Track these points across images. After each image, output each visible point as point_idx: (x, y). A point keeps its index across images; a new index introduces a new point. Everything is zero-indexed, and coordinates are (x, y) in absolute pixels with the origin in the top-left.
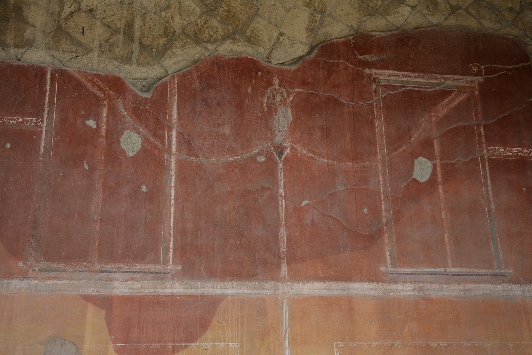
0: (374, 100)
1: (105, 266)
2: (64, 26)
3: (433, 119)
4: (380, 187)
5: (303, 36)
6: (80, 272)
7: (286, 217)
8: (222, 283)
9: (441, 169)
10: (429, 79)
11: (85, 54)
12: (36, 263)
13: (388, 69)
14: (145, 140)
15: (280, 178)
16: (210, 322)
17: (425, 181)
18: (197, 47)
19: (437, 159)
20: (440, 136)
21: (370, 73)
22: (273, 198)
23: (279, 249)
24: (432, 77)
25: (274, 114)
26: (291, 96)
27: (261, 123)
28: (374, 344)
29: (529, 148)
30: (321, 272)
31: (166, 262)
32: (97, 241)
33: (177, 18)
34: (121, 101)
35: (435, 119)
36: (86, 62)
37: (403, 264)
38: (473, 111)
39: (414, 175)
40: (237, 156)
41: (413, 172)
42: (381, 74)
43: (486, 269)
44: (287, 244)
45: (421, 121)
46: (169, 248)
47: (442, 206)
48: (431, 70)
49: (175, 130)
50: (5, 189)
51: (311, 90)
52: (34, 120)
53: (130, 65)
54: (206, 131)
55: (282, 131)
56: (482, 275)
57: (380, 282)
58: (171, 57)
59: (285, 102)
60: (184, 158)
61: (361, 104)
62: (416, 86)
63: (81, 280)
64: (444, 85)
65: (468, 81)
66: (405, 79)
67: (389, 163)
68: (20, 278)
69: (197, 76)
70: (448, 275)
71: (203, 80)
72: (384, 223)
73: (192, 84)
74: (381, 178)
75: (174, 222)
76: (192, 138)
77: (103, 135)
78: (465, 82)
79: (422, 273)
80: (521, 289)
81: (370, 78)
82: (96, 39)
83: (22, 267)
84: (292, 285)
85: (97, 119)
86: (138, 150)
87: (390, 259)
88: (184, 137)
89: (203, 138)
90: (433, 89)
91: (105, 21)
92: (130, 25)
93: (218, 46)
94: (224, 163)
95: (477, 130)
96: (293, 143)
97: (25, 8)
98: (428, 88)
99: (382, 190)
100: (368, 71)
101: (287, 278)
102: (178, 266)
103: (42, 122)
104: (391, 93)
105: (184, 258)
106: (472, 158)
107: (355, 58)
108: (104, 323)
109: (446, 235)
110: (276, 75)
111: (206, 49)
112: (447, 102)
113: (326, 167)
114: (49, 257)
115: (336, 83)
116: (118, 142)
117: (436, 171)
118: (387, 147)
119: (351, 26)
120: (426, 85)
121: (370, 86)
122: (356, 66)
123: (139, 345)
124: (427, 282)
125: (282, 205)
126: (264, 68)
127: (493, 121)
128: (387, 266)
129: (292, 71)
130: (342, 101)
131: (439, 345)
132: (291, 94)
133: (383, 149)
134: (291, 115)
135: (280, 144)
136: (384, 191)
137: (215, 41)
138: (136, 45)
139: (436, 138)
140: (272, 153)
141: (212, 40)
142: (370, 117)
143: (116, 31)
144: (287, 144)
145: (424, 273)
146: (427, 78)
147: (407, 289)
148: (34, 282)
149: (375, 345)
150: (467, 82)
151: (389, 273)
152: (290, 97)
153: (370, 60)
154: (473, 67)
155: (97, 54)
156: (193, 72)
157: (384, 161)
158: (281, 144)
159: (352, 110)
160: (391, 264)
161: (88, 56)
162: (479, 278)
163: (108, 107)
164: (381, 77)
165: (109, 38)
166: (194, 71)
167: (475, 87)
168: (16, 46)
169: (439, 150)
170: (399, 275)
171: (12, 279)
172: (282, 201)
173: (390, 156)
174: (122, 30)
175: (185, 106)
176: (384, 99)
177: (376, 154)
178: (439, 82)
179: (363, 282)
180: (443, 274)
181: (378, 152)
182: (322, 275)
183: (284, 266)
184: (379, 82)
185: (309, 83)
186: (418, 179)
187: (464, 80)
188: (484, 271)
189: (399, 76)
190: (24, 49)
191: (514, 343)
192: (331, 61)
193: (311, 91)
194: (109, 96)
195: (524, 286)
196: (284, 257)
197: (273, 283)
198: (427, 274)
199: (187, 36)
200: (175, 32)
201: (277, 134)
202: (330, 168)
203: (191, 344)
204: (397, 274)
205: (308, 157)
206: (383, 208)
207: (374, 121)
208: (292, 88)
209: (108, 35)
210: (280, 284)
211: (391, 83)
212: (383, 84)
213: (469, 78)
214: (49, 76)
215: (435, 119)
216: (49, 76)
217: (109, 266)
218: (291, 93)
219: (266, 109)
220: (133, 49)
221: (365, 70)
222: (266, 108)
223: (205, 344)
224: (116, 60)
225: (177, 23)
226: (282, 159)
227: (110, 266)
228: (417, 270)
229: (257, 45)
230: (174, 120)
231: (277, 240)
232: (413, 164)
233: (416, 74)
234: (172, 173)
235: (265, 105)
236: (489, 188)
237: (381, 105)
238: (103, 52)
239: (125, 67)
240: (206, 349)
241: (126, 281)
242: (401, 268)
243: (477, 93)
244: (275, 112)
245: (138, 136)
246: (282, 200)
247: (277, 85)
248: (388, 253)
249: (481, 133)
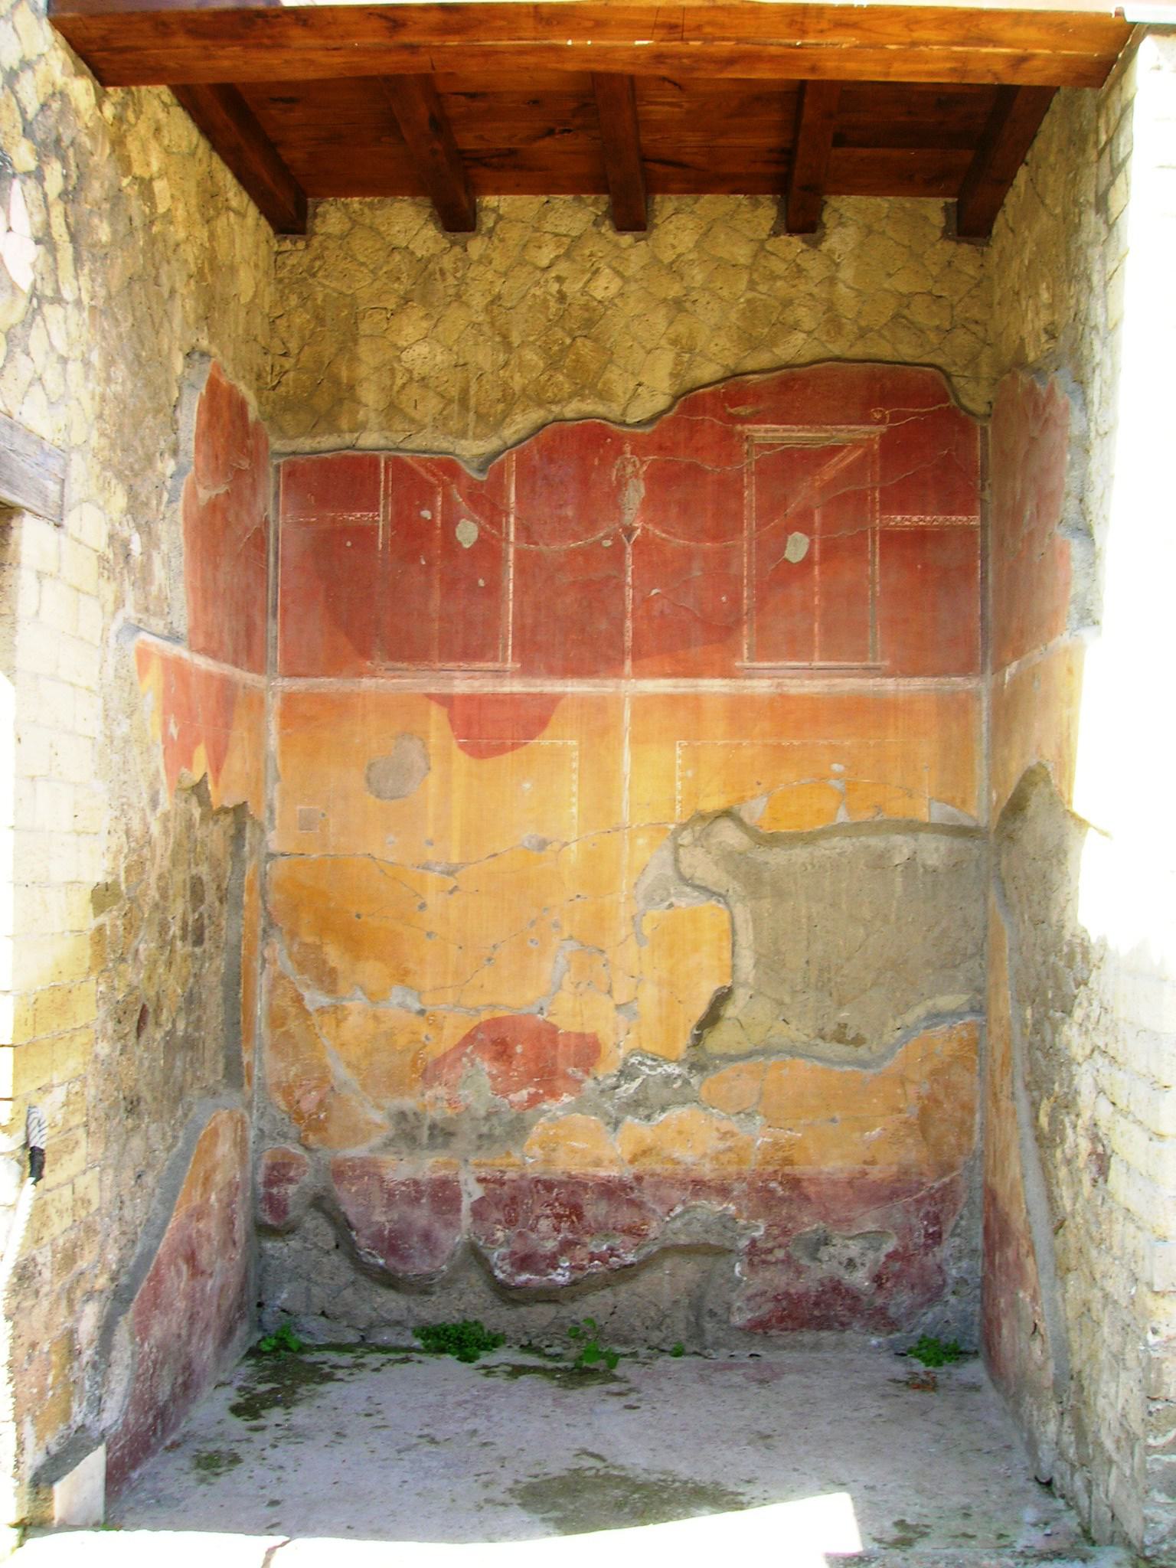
3: (817, 484)
14: (482, 529)
22: (620, 587)
31: (505, 660)
33: (517, 377)
37: (761, 659)
66: (785, 434)
85: (432, 509)
92: (465, 392)
100: (739, 427)
108: (446, 720)
109: (816, 625)
111: (550, 411)
114: (393, 657)
137: (559, 402)
143: (450, 401)
162: (849, 672)
165: (444, 409)
168: (351, 431)
176: (757, 462)
177: (741, 531)
183: (628, 663)
187: (862, 432)
205: (663, 539)
213: (867, 428)
219: (615, 483)
225: (518, 382)
227: (451, 665)
231: (621, 634)
232: (786, 541)
234: (511, 563)
243: (876, 447)
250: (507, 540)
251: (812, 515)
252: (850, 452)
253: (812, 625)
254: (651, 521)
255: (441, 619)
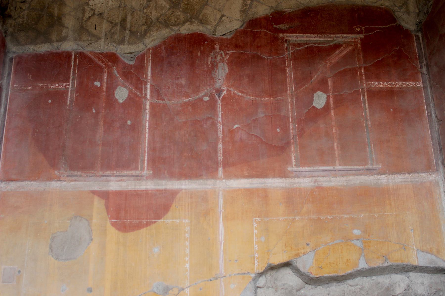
0: (286, 54)
1: (105, 173)
2: (85, 25)
3: (328, 65)
4: (289, 113)
5: (238, 15)
6: (90, 176)
7: (222, 137)
8: (178, 182)
9: (333, 99)
10: (325, 38)
11: (97, 41)
12: (65, 171)
13: (296, 33)
14: (130, 92)
15: (219, 111)
16: (171, 206)
17: (321, 107)
18: (167, 29)
19: (331, 92)
20: (333, 77)
21: (283, 36)
22: (214, 125)
23: (217, 158)
24: (327, 37)
25: (216, 68)
26: (227, 55)
27: (206, 75)
28: (282, 218)
29: (395, 82)
30: (246, 172)
31: (143, 169)
32: (100, 157)
33: (154, 13)
34: (116, 68)
35: (329, 65)
36: (97, 46)
38: (357, 58)
39: (313, 104)
40: (190, 98)
41: (313, 102)
42: (291, 37)
43: (363, 166)
44: (223, 154)
45: (319, 67)
46: (144, 160)
47: (333, 124)
48: (327, 31)
49: (149, 84)
50: (48, 128)
51: (241, 51)
52: (64, 84)
53: (124, 45)
54: (170, 83)
55: (221, 79)
56: (360, 170)
57: (288, 177)
58: (149, 37)
59: (223, 60)
60: (155, 101)
61: (277, 58)
62: (316, 43)
63: (90, 181)
64: (336, 42)
65: (353, 38)
66: (308, 39)
67: (296, 97)
68: (56, 181)
69: (164, 47)
70: (335, 171)
71: (168, 50)
72: (291, 138)
73: (161, 53)
74: (290, 107)
75: (148, 143)
76: (160, 88)
77: (104, 91)
78: (351, 39)
79: (317, 170)
80: (386, 178)
81: (283, 40)
82: (103, 31)
83: (57, 174)
84: (226, 181)
85: (101, 81)
86: (126, 98)
87: (295, 162)
88: (155, 88)
89: (168, 87)
90: (328, 45)
91: (109, 19)
92: (124, 20)
93: (180, 28)
94: (181, 103)
95: (359, 71)
96: (228, 87)
97: (63, 19)
98: (324, 44)
99: (290, 115)
100: (281, 35)
101: (222, 177)
102: (150, 172)
103: (69, 85)
104: (298, 49)
105: (154, 166)
106: (355, 90)
107: (272, 27)
109: (335, 144)
110: (217, 43)
111: (172, 30)
112: (338, 53)
113: (251, 101)
114: (72, 168)
115: (259, 45)
116: (114, 94)
117: (330, 100)
118: (294, 86)
119: (272, 6)
120: (323, 42)
121: (283, 45)
122: (273, 33)
123: (126, 221)
124: (320, 177)
125: (220, 129)
126: (209, 39)
127: (371, 64)
128: (292, 167)
129: (228, 39)
130: (263, 56)
131: (327, 218)
132: (228, 54)
133: (292, 87)
134: (227, 68)
135: (219, 88)
136: (292, 116)
137: (178, 25)
138: (128, 32)
139: (330, 78)
140: (214, 94)
141: (176, 24)
142: (283, 66)
143: (116, 24)
144: (224, 88)
145: (319, 170)
146: (323, 37)
147: (306, 181)
148: (64, 183)
149: (282, 220)
150: (352, 38)
151: (294, 171)
152: (227, 56)
153: (283, 28)
154: (356, 28)
155: (103, 40)
156: (162, 46)
157: (292, 95)
158: (220, 88)
159: (270, 62)
160: (295, 165)
161: (98, 42)
162: (358, 173)
163: (107, 73)
164: (290, 39)
165: (112, 29)
166: (162, 45)
167: (358, 42)
168: (57, 41)
169: (332, 86)
170: (301, 172)
171: (52, 181)
172: (220, 126)
173: (297, 92)
174: (119, 23)
175: (156, 67)
176: (293, 53)
177: (286, 91)
178: (332, 39)
179: (275, 178)
180: (332, 171)
181: (288, 89)
182: (247, 174)
183: (221, 170)
184: (289, 42)
185: (240, 46)
186: (317, 107)
187: (350, 37)
188: (361, 167)
189: (304, 37)
190: (62, 43)
191: (379, 214)
192: (255, 31)
193: (241, 52)
194: (108, 66)
195: (389, 176)
196: (221, 163)
197: (213, 180)
198: (321, 171)
199: (160, 23)
200: (152, 21)
201: (217, 81)
202: (254, 102)
203: (158, 220)
204: (299, 171)
205: (239, 96)
206: (291, 128)
207: (285, 68)
208: (228, 51)
209: (110, 27)
210: (218, 181)
211: (298, 42)
212: (292, 43)
213: (353, 36)
214: (73, 57)
215: (329, 65)
216: (73, 57)
217: (107, 172)
218: (227, 54)
219: (210, 66)
220: (126, 35)
221: (279, 35)
222: (210, 65)
223: (167, 220)
224: (115, 43)
225: (154, 15)
226: (221, 98)
227: (108, 173)
228: (314, 169)
229: (206, 24)
230: (149, 77)
231: (216, 152)
232: (313, 97)
233: (316, 35)
234: (147, 111)
235: (209, 63)
236: (367, 110)
237: (291, 57)
238: (107, 39)
239: (121, 46)
240: (167, 224)
241: (117, 182)
242: (302, 168)
243: (359, 45)
244: (216, 67)
245: (126, 89)
246: (220, 125)
247: (218, 49)
248: (293, 158)
249: (362, 72)
250: (145, 98)
251: (328, 81)
252: (345, 48)
253: (334, 144)
254: (232, 86)
255: (103, 144)
